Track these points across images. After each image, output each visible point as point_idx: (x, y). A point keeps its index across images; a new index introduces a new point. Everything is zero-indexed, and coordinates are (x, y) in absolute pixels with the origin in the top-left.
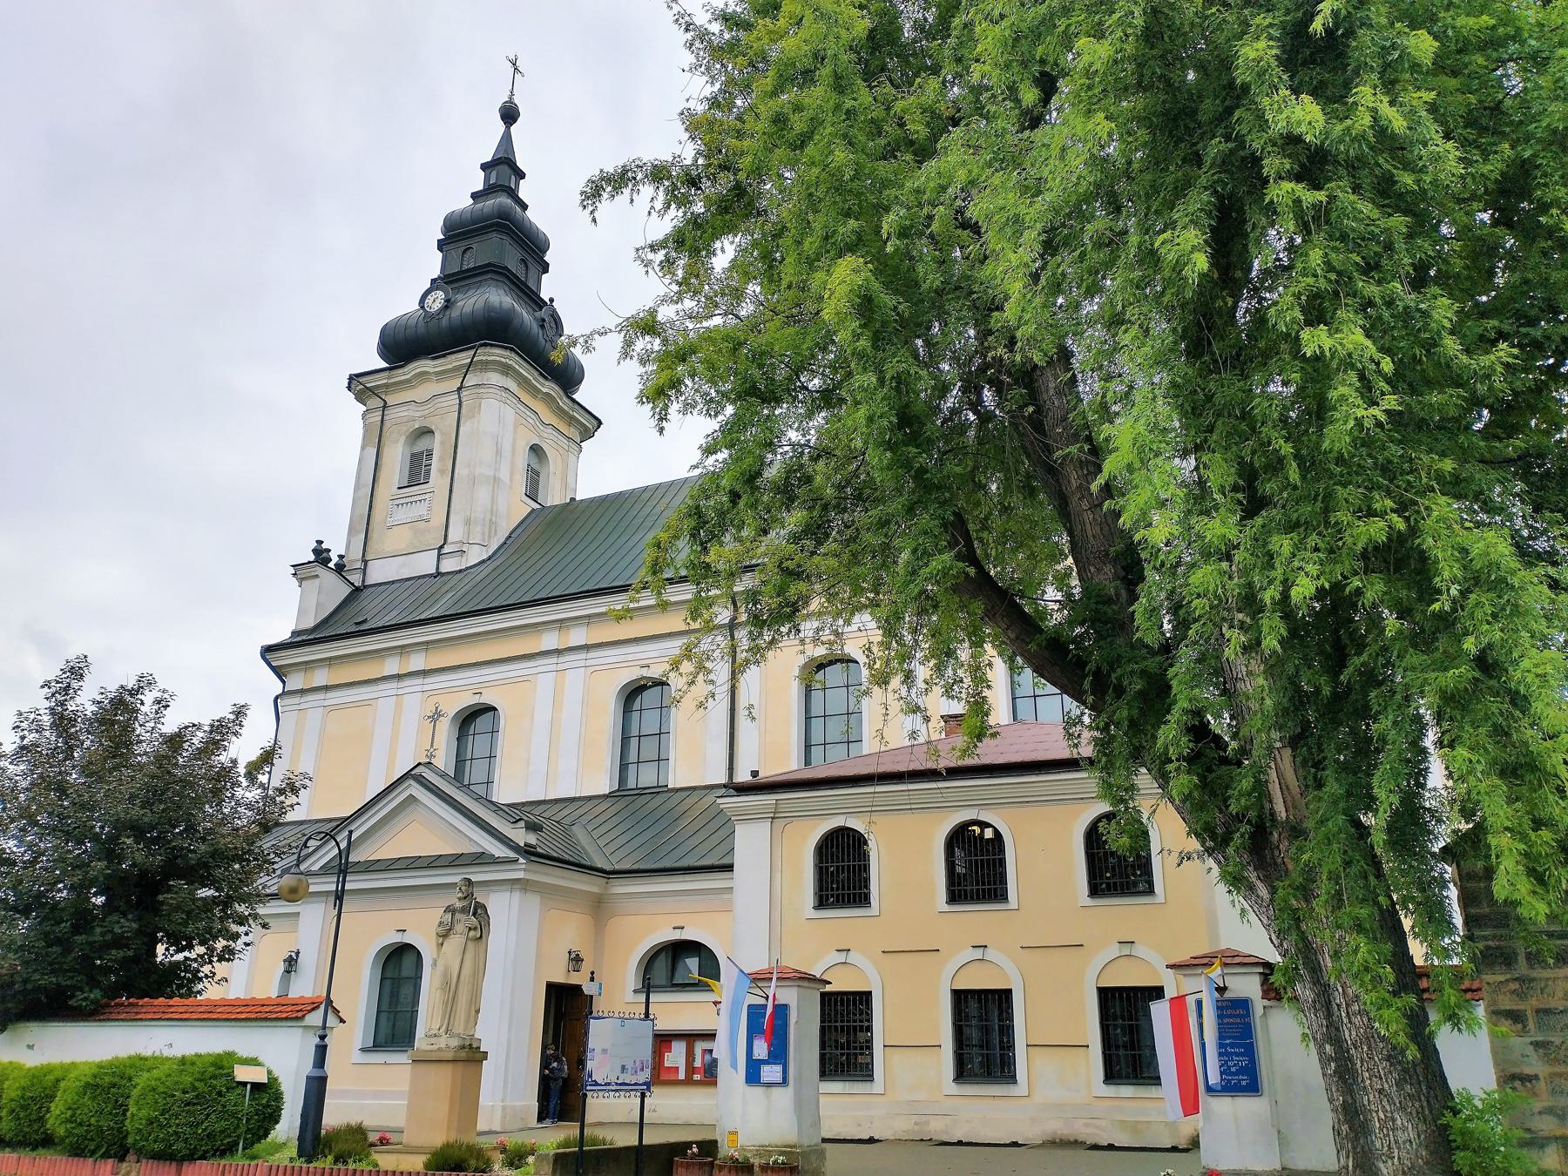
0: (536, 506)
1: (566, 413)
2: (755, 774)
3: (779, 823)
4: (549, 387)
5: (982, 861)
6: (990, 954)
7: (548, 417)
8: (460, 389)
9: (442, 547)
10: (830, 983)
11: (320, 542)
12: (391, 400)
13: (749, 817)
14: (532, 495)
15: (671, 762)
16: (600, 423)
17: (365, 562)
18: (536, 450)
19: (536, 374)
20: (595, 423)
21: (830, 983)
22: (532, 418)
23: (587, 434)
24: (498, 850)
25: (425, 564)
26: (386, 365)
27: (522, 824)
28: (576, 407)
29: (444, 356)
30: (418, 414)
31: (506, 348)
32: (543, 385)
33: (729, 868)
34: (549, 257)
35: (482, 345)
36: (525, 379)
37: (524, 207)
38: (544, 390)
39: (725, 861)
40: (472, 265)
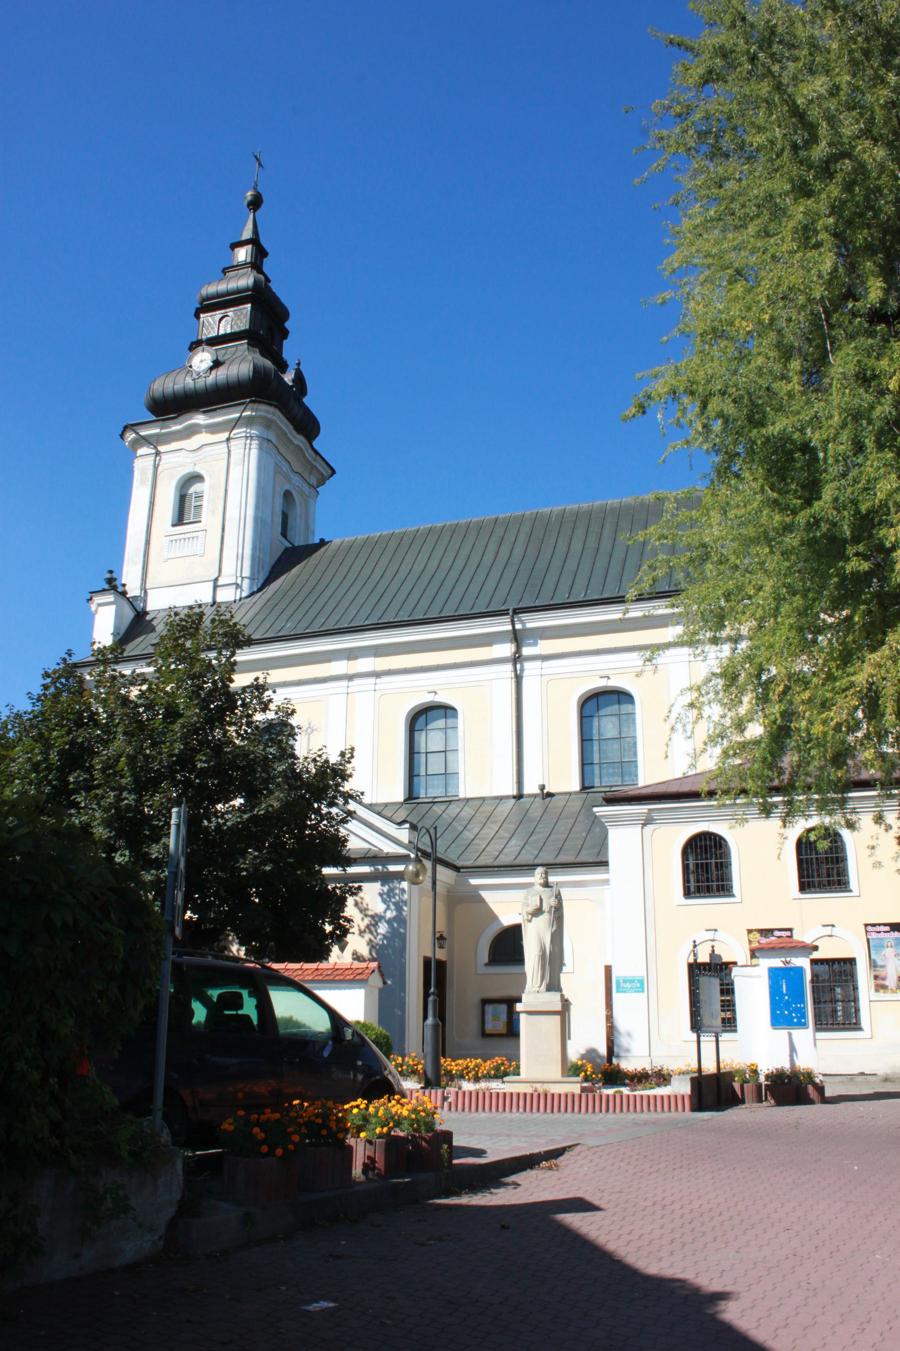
0: (289, 545)
1: (310, 463)
2: (542, 787)
3: (649, 828)
4: (299, 440)
5: (702, 864)
6: (835, 931)
7: (298, 468)
8: (228, 439)
9: (216, 580)
10: (816, 948)
11: (111, 572)
12: (161, 448)
13: (618, 821)
14: (284, 534)
15: (461, 776)
16: (334, 472)
17: (146, 592)
18: (287, 495)
19: (291, 427)
20: (330, 472)
21: (816, 948)
22: (285, 468)
23: (322, 481)
24: (389, 848)
25: (202, 595)
26: (155, 418)
27: (407, 825)
28: (318, 458)
29: (215, 410)
30: (189, 460)
31: (271, 405)
32: (295, 438)
33: (604, 864)
34: (287, 325)
35: (251, 402)
36: (284, 434)
37: (268, 280)
38: (296, 442)
39: (603, 860)
40: (229, 331)
